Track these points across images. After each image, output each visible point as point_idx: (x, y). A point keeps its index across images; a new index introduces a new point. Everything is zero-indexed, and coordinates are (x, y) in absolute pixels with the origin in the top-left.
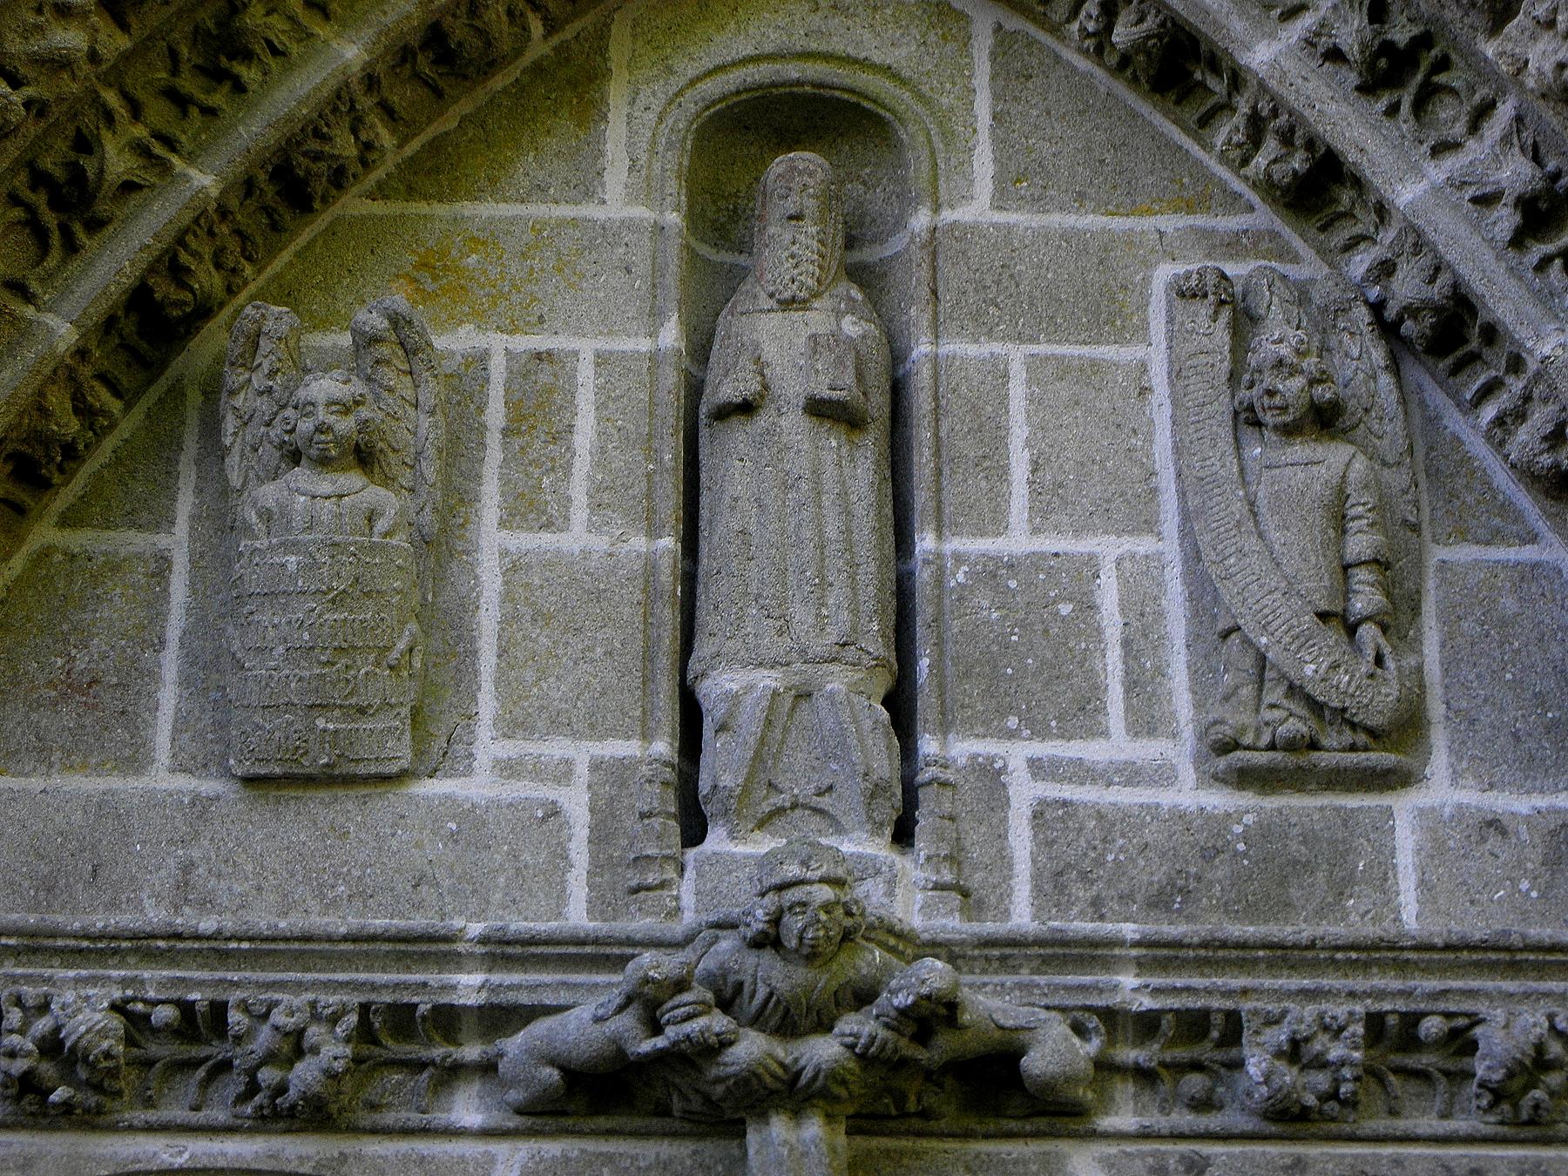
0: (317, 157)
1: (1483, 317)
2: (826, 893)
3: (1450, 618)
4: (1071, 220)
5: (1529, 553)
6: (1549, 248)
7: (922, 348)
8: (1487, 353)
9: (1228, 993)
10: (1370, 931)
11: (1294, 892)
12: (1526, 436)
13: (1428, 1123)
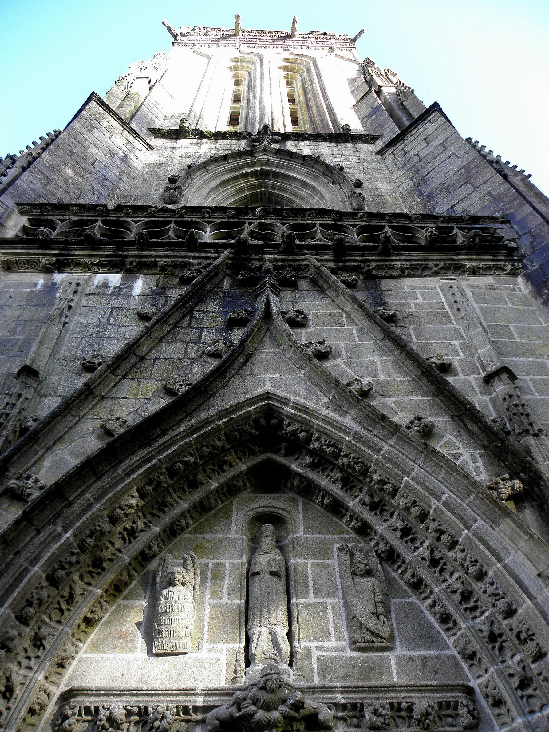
0: (178, 525)
1: (397, 552)
2: (275, 676)
3: (397, 614)
4: (318, 536)
5: (410, 600)
6: (407, 538)
7: (292, 561)
8: (398, 560)
9: (360, 699)
10: (389, 683)
11: (372, 675)
12: (407, 576)
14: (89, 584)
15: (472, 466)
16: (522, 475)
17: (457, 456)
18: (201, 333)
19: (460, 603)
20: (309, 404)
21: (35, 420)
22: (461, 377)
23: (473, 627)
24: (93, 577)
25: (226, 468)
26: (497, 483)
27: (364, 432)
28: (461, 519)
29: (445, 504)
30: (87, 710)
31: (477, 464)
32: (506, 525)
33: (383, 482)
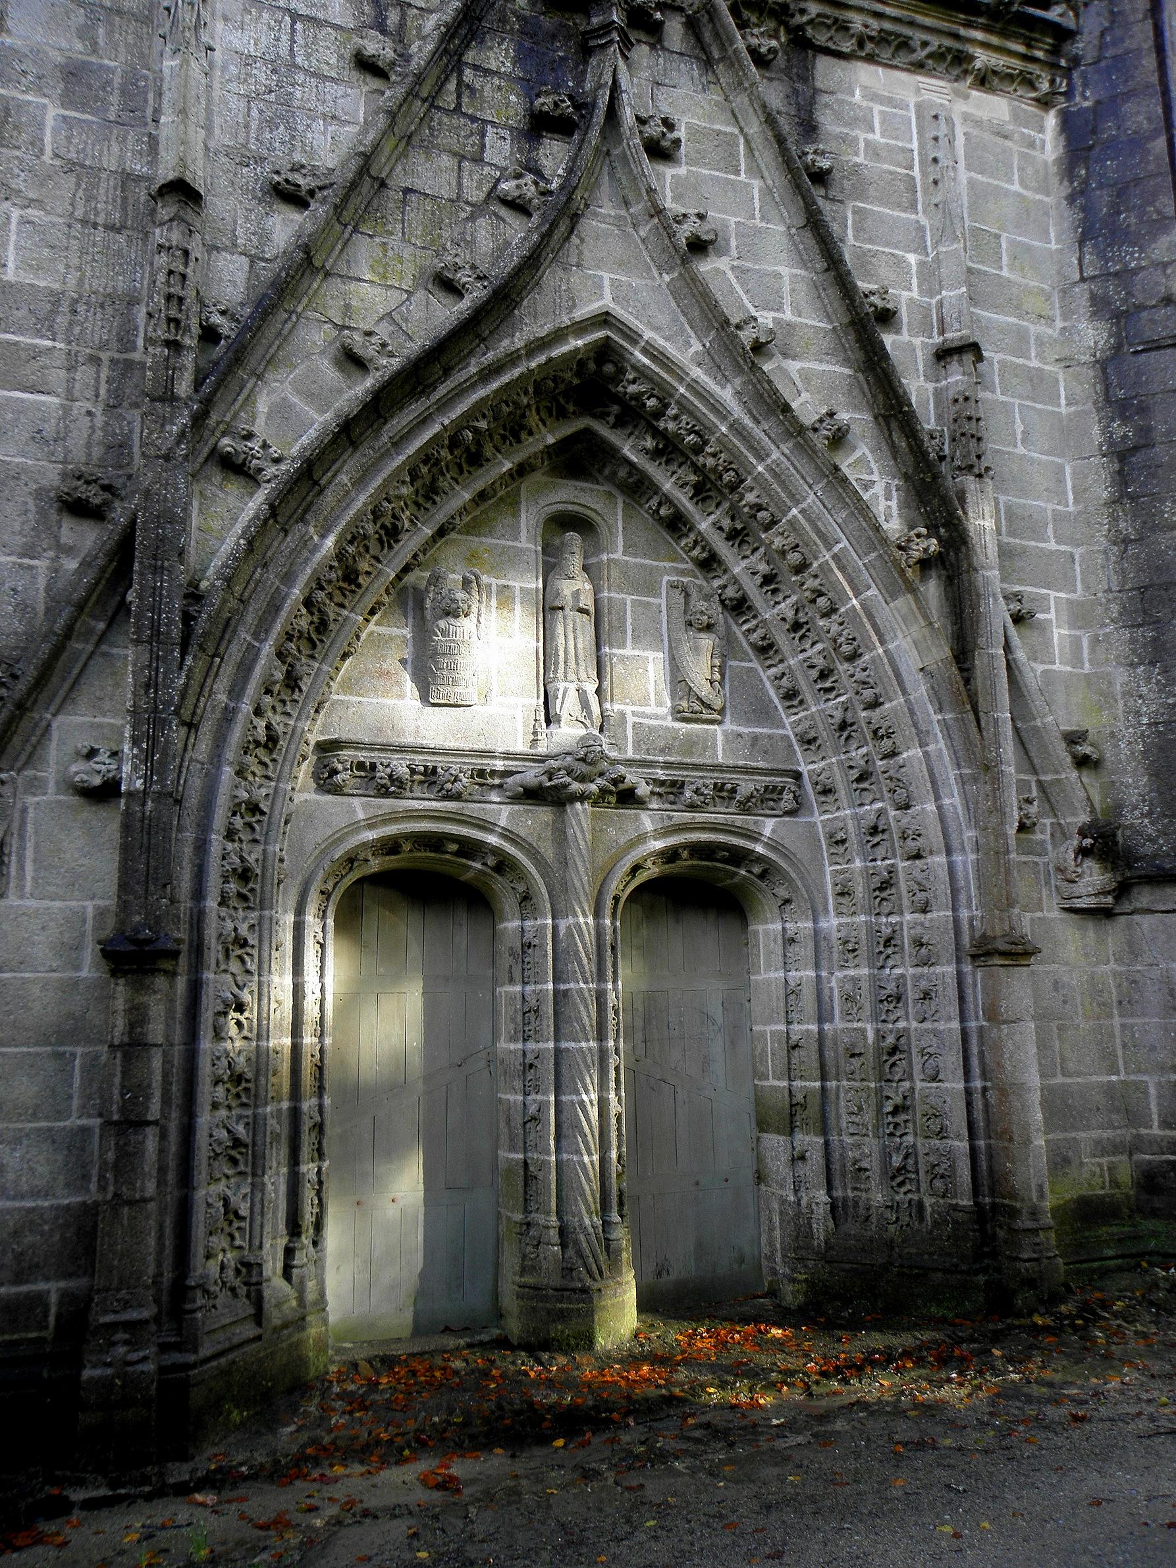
5: (750, 665)
12: (755, 637)
13: (723, 810)
14: (342, 606)
16: (942, 530)
17: (867, 486)
18: (483, 135)
20: (671, 349)
21: (223, 313)
22: (905, 336)
23: (823, 711)
24: (345, 596)
25: (524, 435)
26: (909, 541)
27: (748, 422)
28: (851, 582)
29: (835, 557)
30: (361, 766)
32: (904, 602)
33: (760, 508)
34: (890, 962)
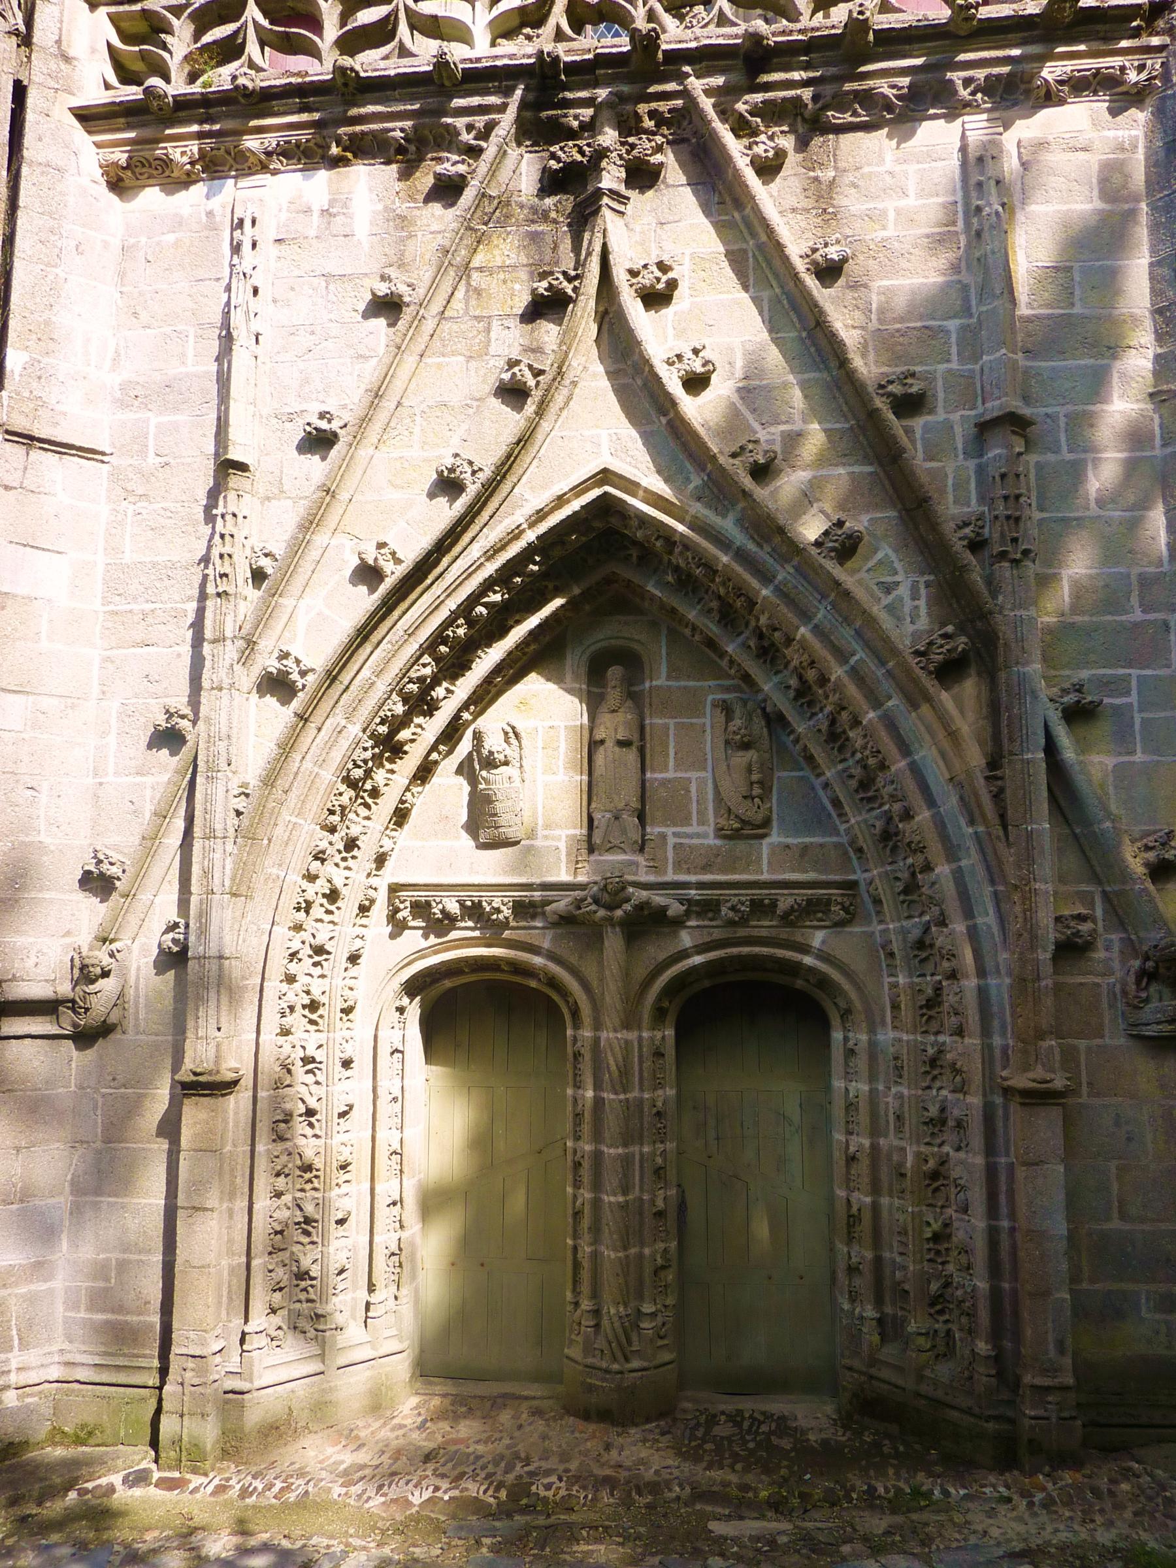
7: (647, 722)
15: (908, 604)
17: (888, 589)
18: (488, 330)
19: (857, 791)
22: (941, 416)
27: (751, 546)
31: (917, 603)
34: (938, 1084)
